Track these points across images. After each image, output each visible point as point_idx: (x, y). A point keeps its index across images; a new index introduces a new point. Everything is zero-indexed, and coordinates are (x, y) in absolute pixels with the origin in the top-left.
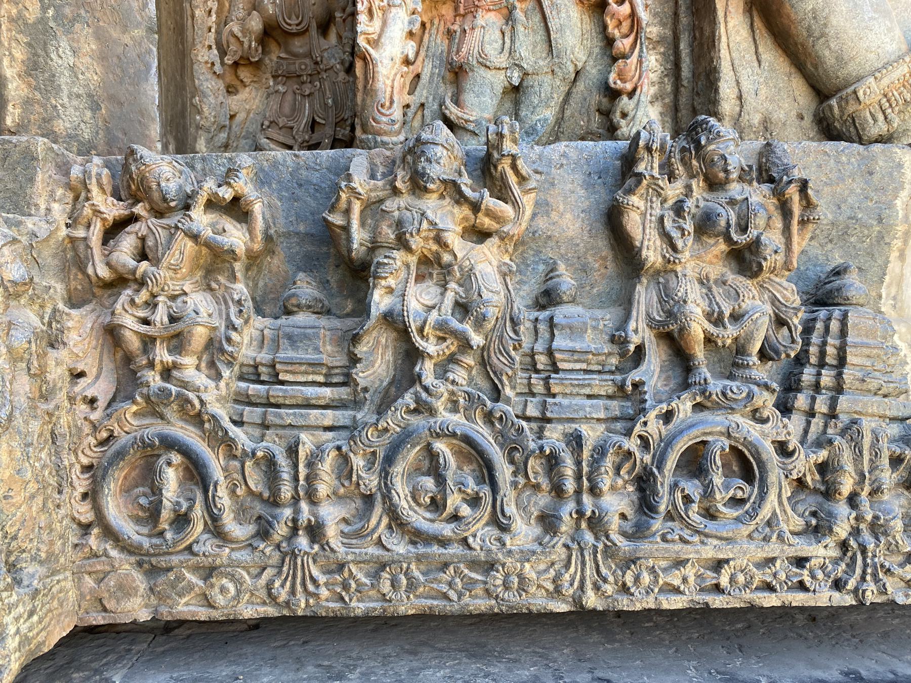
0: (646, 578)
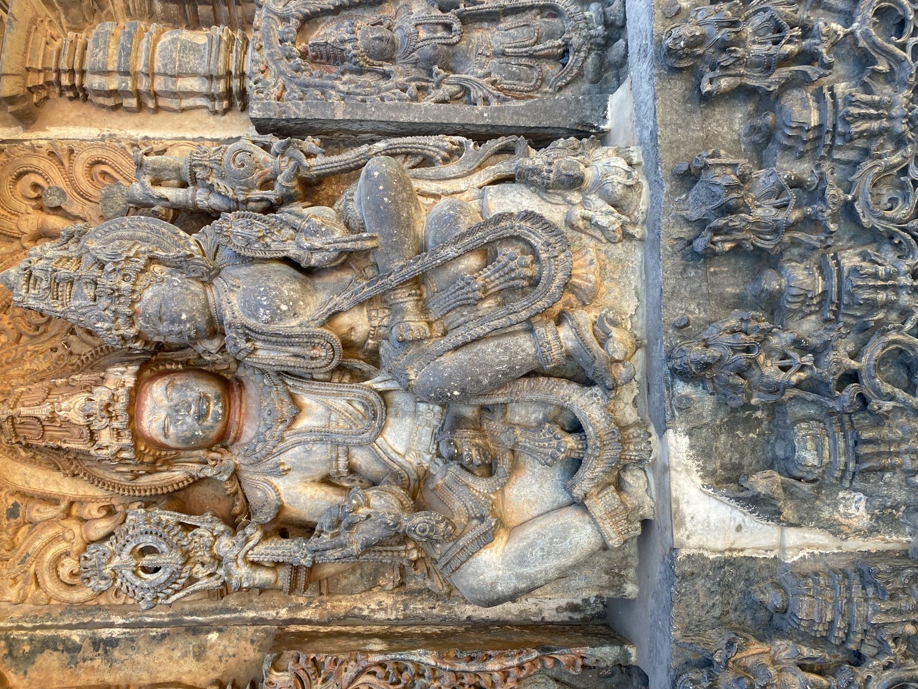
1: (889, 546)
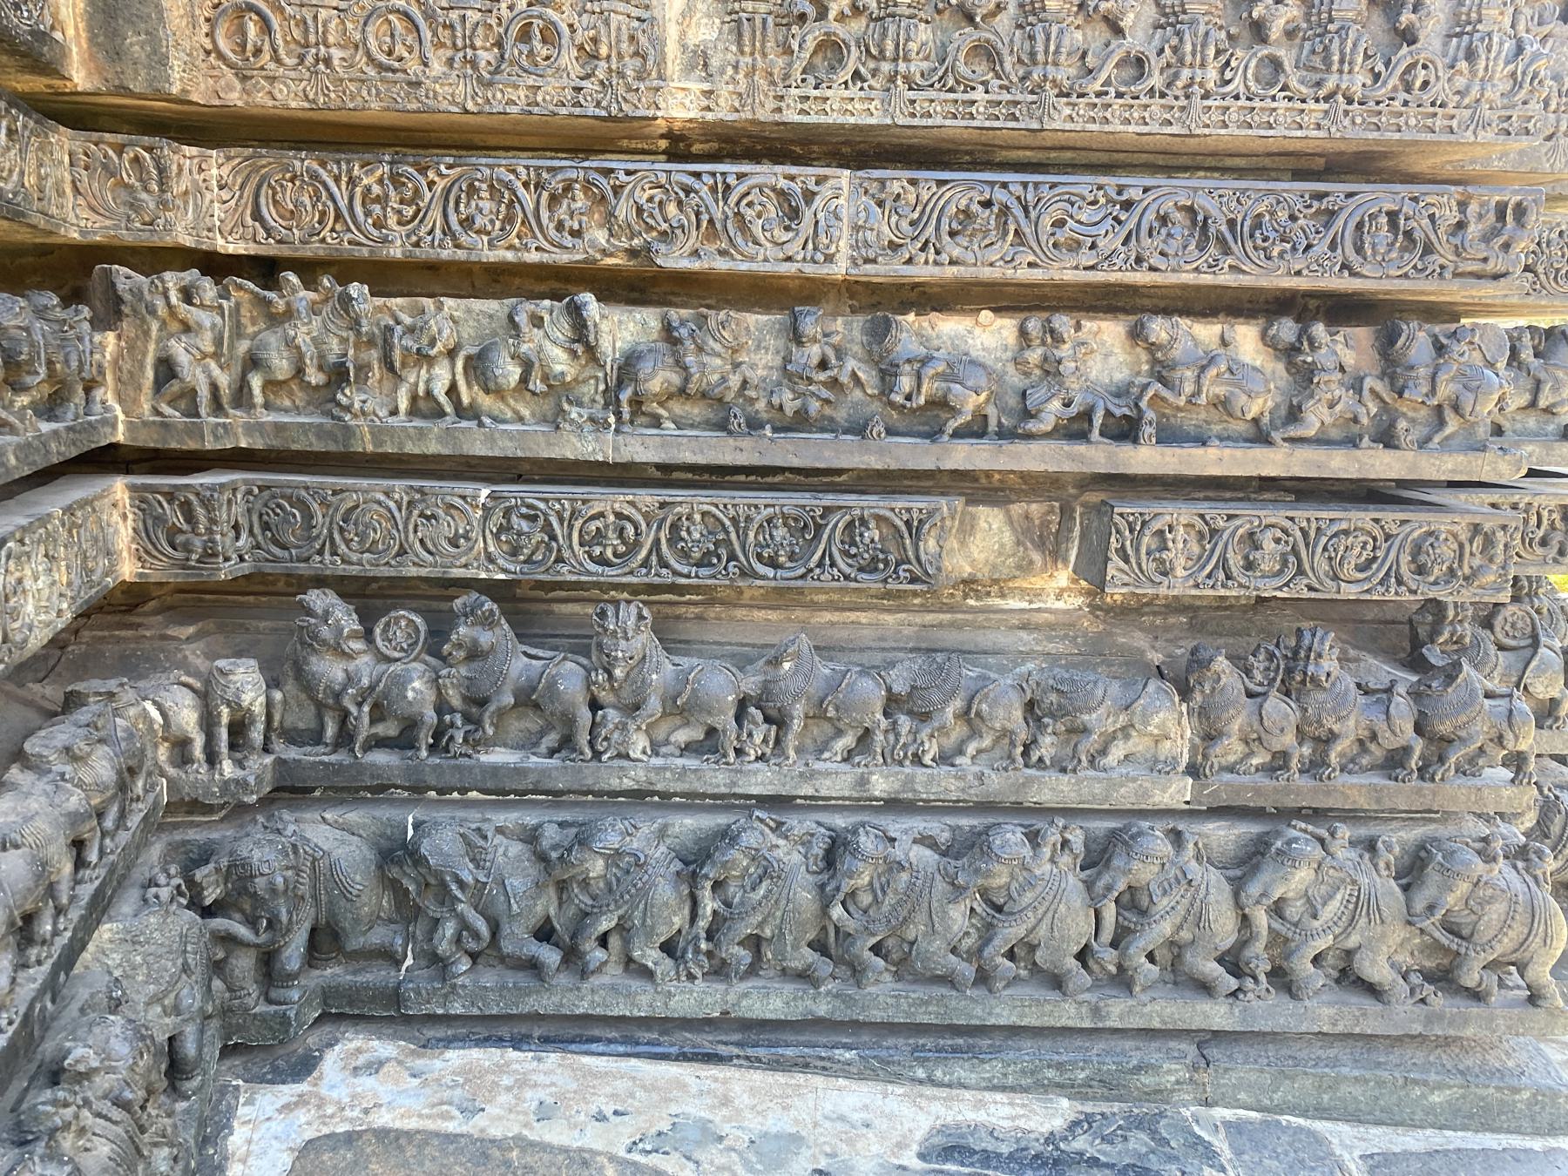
0: (499, 95)
1: (669, 64)
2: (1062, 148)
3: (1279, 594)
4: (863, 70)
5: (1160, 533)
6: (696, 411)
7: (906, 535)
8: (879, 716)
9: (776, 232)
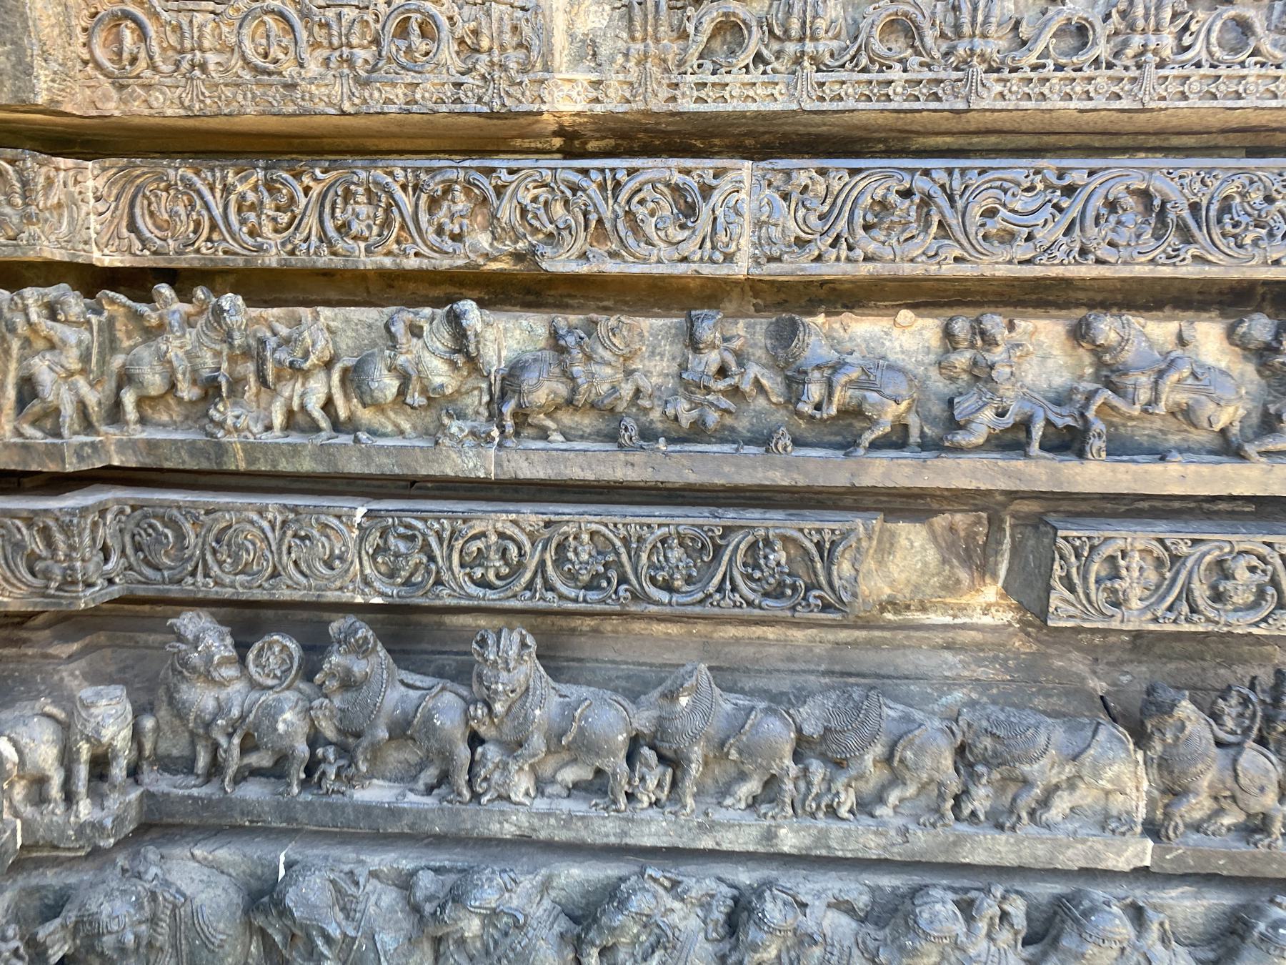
0: (376, 94)
1: (557, 55)
2: (988, 132)
3: (1255, 631)
4: (765, 52)
5: (1112, 558)
6: (586, 421)
7: (817, 559)
8: (788, 762)
9: (671, 231)
